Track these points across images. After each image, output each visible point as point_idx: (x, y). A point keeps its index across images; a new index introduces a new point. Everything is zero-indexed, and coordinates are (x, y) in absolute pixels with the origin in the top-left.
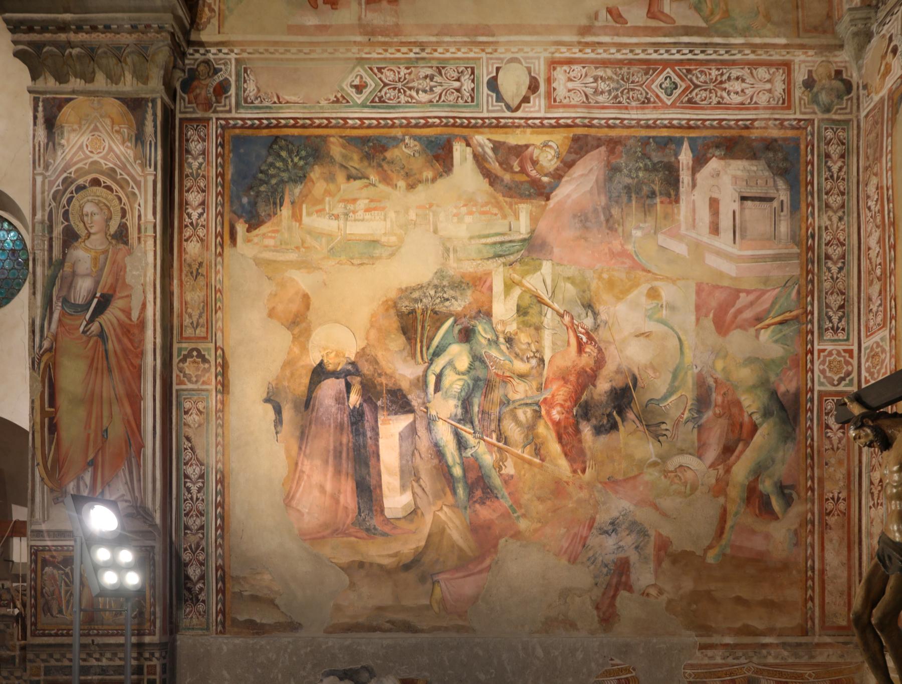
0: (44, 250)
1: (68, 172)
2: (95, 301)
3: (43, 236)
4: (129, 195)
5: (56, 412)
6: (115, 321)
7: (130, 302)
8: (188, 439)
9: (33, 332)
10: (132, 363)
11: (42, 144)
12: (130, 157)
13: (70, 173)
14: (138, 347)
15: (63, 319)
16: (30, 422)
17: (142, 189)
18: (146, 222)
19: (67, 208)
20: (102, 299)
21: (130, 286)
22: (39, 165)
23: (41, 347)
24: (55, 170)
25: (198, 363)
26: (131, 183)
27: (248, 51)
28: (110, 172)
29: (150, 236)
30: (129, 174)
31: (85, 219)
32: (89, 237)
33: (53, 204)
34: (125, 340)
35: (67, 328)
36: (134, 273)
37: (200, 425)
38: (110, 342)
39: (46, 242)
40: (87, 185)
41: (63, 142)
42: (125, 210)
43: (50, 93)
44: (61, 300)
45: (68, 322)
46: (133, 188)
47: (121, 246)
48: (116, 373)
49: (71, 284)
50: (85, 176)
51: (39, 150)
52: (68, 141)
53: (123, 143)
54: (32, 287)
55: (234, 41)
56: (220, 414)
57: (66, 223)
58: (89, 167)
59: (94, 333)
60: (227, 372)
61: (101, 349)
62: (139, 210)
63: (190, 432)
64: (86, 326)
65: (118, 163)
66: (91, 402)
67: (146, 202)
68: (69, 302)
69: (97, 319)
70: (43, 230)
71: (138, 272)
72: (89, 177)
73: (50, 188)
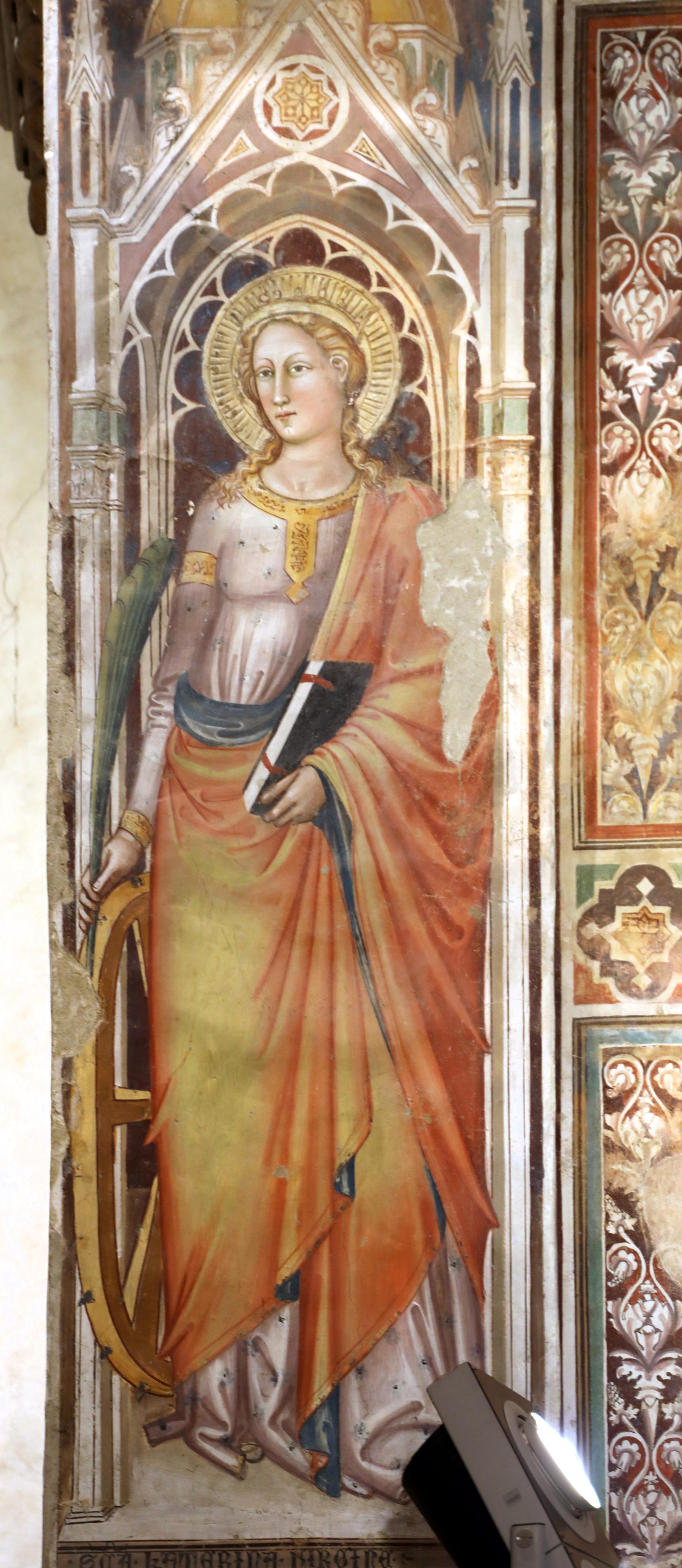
0: (106, 507)
1: (197, 210)
2: (304, 690)
3: (105, 453)
4: (432, 290)
5: (155, 1105)
6: (378, 764)
7: (437, 693)
9: (69, 812)
10: (446, 920)
11: (94, 105)
12: (436, 146)
13: (205, 216)
14: (469, 858)
15: (177, 759)
16: (55, 1143)
17: (484, 269)
18: (500, 392)
19: (193, 347)
20: (328, 685)
21: (436, 631)
22: (85, 188)
23: (97, 866)
24: (147, 203)
25: (658, 921)
28: (358, 209)
29: (516, 444)
30: (433, 214)
31: (263, 386)
32: (276, 455)
33: (142, 334)
34: (420, 835)
35: (195, 793)
36: (454, 583)
38: (360, 840)
39: (113, 478)
40: (270, 258)
41: (175, 95)
42: (416, 347)
44: (171, 689)
45: (200, 770)
46: (445, 265)
47: (402, 485)
48: (385, 957)
49: (210, 628)
50: (263, 223)
51: (85, 130)
52: (194, 93)
53: (408, 93)
54: (60, 647)
57: (191, 406)
58: (275, 191)
59: (296, 811)
61: (325, 870)
62: (471, 349)
64: (268, 784)
65: (390, 170)
66: (293, 1065)
67: (497, 317)
68: (200, 698)
69: (310, 759)
70: (104, 430)
71: (468, 581)
73: (129, 274)
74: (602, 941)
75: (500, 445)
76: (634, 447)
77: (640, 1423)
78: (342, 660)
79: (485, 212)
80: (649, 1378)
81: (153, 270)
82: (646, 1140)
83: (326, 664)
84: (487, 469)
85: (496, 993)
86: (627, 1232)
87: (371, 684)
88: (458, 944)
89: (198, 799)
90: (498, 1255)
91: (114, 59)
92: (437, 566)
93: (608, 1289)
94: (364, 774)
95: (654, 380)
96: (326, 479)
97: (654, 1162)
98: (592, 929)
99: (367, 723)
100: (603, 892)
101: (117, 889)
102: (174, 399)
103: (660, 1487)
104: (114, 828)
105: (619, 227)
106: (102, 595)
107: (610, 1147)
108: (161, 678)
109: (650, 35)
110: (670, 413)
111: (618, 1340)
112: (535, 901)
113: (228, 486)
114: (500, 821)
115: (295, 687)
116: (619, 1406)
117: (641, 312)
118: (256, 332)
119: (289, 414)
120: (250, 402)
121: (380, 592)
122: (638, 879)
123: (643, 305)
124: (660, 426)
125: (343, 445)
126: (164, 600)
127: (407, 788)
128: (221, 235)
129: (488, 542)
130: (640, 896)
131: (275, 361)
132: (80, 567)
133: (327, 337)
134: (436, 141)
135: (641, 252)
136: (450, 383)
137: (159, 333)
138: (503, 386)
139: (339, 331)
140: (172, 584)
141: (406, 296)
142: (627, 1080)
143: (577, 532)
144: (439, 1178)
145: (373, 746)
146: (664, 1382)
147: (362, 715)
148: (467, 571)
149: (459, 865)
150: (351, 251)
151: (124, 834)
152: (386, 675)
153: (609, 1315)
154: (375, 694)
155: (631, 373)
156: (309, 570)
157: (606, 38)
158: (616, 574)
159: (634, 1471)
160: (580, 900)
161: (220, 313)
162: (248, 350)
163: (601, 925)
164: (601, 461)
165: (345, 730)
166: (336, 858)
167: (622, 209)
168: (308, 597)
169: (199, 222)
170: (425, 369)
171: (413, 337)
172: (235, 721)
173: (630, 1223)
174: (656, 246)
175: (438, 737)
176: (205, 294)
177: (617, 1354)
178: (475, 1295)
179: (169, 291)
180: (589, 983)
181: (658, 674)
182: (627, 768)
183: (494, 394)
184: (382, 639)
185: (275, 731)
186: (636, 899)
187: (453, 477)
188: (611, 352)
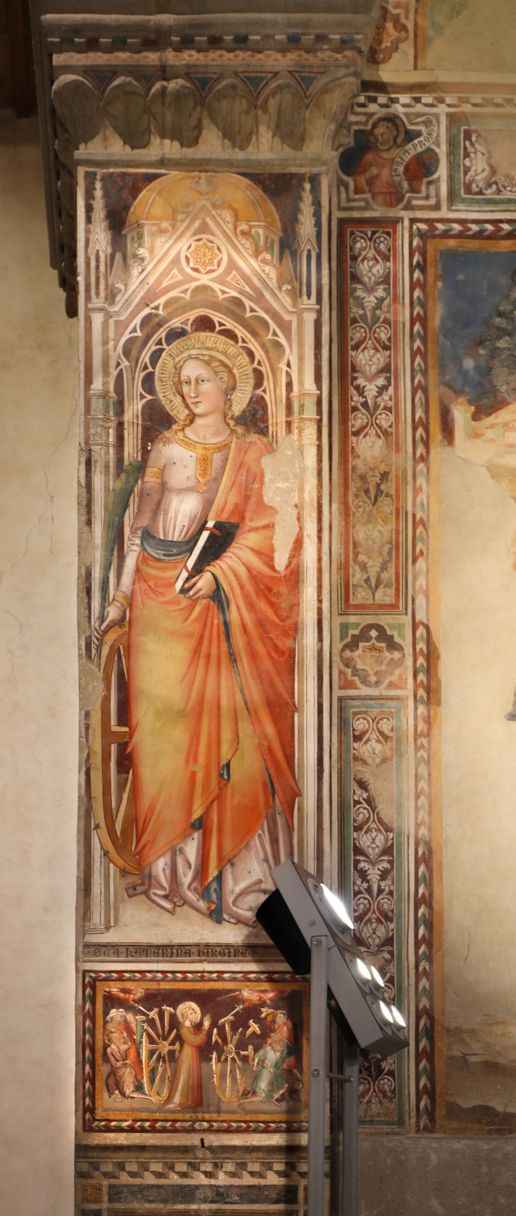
0: (107, 445)
1: (153, 305)
2: (205, 535)
4: (269, 346)
5: (131, 734)
6: (242, 571)
7: (272, 538)
8: (362, 785)
9: (89, 591)
10: (276, 647)
11: (102, 256)
12: (271, 279)
13: (157, 308)
16: (81, 751)
18: (302, 395)
19: (150, 369)
20: (217, 532)
21: (271, 508)
22: (97, 294)
23: (102, 618)
24: (128, 302)
26: (273, 325)
27: (473, 101)
28: (232, 307)
29: (310, 420)
30: (268, 310)
31: (185, 389)
32: (192, 422)
33: (125, 363)
34: (263, 605)
35: (151, 583)
36: (280, 485)
37: (384, 761)
38: (233, 608)
39: (111, 431)
40: (188, 328)
41: (142, 252)
42: (260, 372)
43: (116, 164)
44: (139, 533)
45: (153, 572)
46: (275, 334)
47: (254, 437)
48: (246, 664)
49: (159, 504)
50: (185, 312)
51: (97, 267)
52: (152, 251)
53: (257, 253)
54: (84, 511)
55: (444, 84)
56: (425, 741)
57: (149, 397)
58: (191, 297)
59: (201, 593)
60: (436, 665)
61: (216, 622)
62: (288, 374)
63: (366, 773)
64: (187, 580)
65: (247, 289)
66: (199, 716)
67: (301, 359)
68: (154, 538)
69: (208, 568)
70: (107, 408)
71: (287, 484)
72: (193, 315)
73: (119, 335)
74: (352, 659)
75: (302, 420)
76: (367, 423)
77: (369, 890)
78: (224, 521)
79: (295, 310)
80: (374, 869)
81: (131, 333)
82: (373, 755)
83: (216, 522)
84: (296, 431)
85: (301, 683)
86: (364, 799)
87: (239, 532)
88: (282, 659)
89: (153, 586)
90: (300, 810)
91: (112, 234)
92: (271, 476)
93: (354, 826)
94: (235, 575)
95: (377, 392)
96: (216, 434)
97: (378, 766)
98: (348, 653)
99: (237, 551)
100: (353, 636)
101: (112, 629)
102: (141, 394)
103: (378, 920)
104: (111, 600)
105: (359, 320)
106: (105, 487)
107: (356, 758)
108: (134, 527)
109: (374, 233)
110: (385, 408)
111: (358, 851)
112: (320, 639)
113: (168, 436)
114: (303, 600)
115: (201, 533)
116: (359, 882)
117: (370, 360)
118: (182, 363)
119: (198, 402)
120: (179, 396)
121: (243, 489)
122: (370, 630)
123: (372, 357)
124: (380, 414)
125: (225, 417)
126: (136, 490)
127: (257, 584)
128: (164, 317)
129: (297, 466)
130: (371, 638)
131: (191, 377)
132: (95, 474)
133: (217, 366)
134: (270, 276)
135: (370, 332)
136: (278, 390)
137: (134, 363)
138: (304, 392)
139: (223, 364)
140: (140, 482)
141: (256, 348)
142: (364, 727)
143: (340, 463)
144: (272, 772)
145: (240, 563)
146: (381, 871)
147: (234, 547)
148: (286, 480)
149: (282, 621)
150: (229, 326)
151: (115, 603)
152: (246, 528)
153: (354, 839)
154: (240, 537)
155: (366, 389)
156: (208, 477)
157: (352, 233)
158: (359, 484)
159: (365, 913)
160: (342, 639)
161: (164, 354)
162: (178, 371)
163: (352, 651)
164: (351, 430)
165: (226, 554)
166: (221, 616)
167: (361, 312)
168: (208, 490)
169: (153, 311)
170: (265, 383)
171: (259, 367)
172: (171, 549)
173: (365, 795)
174: (378, 330)
175: (272, 559)
176: (157, 344)
177: (358, 858)
178: (290, 828)
179: (139, 343)
180: (346, 680)
181: (380, 532)
182: (365, 576)
183: (300, 396)
184: (244, 511)
185: (191, 554)
186: (369, 639)
187: (279, 435)
188: (356, 378)
